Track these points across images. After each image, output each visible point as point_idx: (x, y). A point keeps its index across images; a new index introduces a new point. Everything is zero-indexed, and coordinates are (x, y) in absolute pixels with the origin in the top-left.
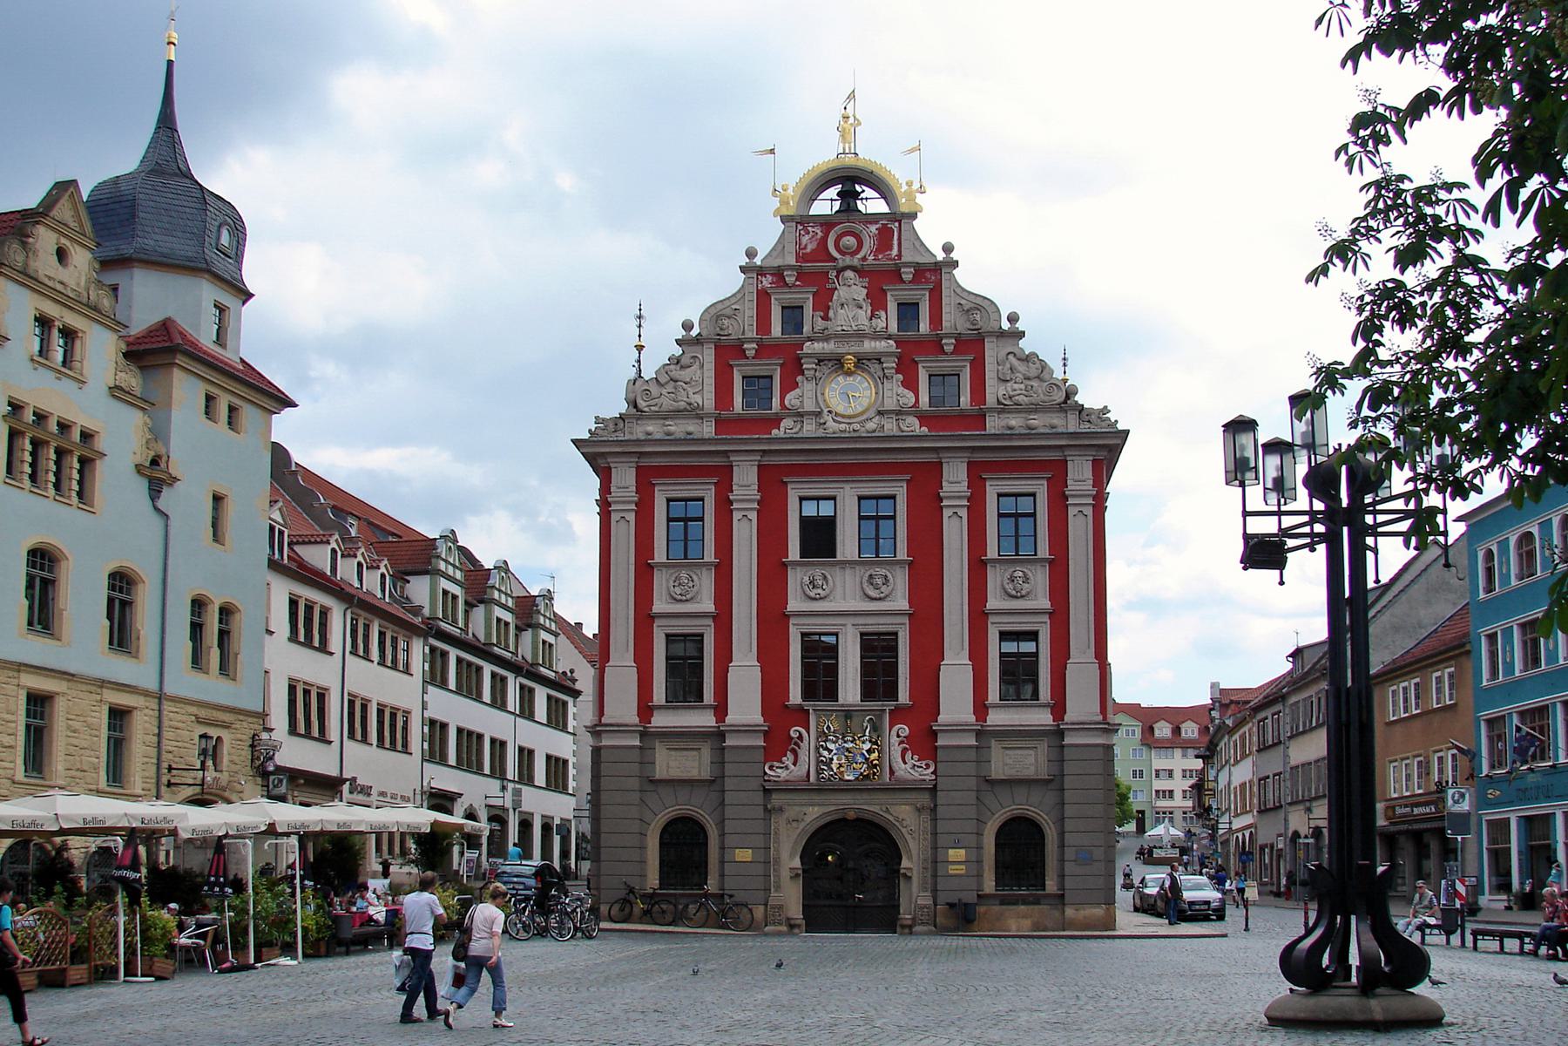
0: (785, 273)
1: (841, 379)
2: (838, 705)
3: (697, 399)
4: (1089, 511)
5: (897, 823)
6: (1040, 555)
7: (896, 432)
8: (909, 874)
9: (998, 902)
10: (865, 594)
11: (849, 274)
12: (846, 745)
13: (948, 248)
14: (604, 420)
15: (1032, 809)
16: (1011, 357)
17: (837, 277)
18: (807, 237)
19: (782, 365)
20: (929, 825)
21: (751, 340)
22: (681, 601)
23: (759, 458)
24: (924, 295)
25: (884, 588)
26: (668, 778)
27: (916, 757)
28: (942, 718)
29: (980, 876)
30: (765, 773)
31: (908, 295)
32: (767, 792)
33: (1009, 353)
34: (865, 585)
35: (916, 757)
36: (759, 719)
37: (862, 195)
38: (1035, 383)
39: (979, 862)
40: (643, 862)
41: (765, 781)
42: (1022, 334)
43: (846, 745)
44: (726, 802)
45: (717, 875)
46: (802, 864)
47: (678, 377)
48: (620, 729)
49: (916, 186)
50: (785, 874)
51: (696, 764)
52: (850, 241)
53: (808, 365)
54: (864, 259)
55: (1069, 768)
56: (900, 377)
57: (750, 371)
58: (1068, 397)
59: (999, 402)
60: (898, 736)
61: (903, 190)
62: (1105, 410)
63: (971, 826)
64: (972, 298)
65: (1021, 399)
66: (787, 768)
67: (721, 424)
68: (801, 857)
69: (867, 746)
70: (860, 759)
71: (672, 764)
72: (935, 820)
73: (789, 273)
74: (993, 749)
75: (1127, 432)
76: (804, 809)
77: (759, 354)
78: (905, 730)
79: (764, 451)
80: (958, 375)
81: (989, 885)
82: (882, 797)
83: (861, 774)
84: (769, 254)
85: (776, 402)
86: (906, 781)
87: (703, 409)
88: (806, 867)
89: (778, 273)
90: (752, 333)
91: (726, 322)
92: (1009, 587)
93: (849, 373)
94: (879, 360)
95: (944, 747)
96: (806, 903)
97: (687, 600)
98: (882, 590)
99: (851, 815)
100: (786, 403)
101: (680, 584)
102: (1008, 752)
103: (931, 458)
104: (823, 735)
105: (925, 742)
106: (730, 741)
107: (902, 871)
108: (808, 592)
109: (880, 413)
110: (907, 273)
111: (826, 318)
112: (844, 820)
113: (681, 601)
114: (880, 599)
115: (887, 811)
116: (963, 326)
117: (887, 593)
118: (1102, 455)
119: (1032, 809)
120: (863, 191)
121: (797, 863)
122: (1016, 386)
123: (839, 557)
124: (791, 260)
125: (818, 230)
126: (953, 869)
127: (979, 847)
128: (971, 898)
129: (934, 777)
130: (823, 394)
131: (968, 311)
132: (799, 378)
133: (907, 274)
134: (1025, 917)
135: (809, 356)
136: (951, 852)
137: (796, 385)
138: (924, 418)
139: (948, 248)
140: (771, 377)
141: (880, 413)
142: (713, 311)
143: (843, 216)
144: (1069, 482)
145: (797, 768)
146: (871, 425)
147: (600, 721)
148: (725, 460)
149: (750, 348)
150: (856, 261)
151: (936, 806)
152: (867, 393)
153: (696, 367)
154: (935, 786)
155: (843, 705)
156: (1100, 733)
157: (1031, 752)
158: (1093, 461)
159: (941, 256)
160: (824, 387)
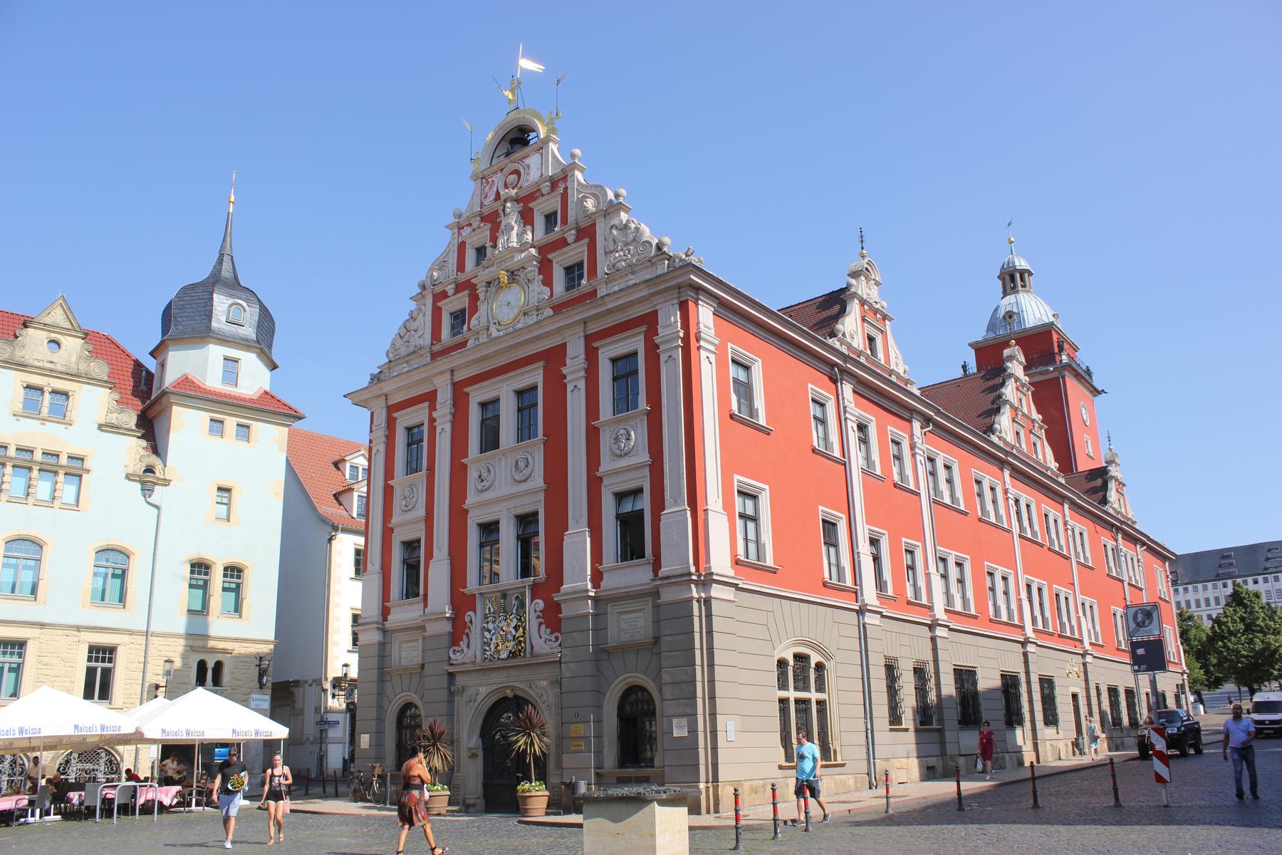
9: (615, 781)
17: (504, 210)
60: (536, 611)
69: (513, 624)
78: (540, 604)
95: (567, 618)
102: (624, 616)
105: (552, 618)
117: (528, 474)
157: (640, 614)
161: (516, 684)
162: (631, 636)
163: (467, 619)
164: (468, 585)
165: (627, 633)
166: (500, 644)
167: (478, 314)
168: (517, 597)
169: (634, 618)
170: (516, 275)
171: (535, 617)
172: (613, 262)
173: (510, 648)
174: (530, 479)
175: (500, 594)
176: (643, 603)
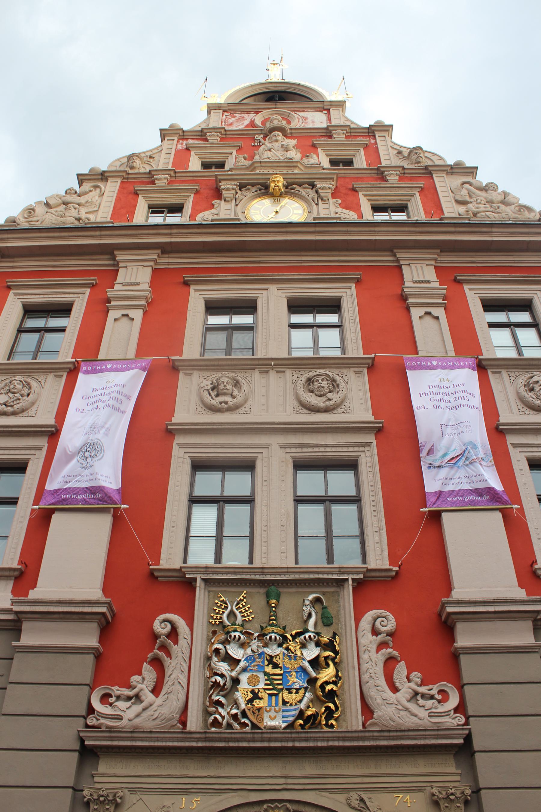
18: (233, 119)
24: (358, 151)
27: (416, 676)
30: (91, 710)
41: (87, 726)
43: (268, 651)
60: (375, 632)
69: (312, 652)
70: (297, 681)
86: (402, 732)
94: (313, 186)
117: (339, 400)
129: (462, 720)
132: (216, 202)
145: (159, 701)
154: (468, 738)
155: (262, 570)
164: (161, 562)
166: (264, 695)
168: (318, 600)
170: (293, 189)
171: (374, 647)
173: (302, 706)
174: (339, 410)
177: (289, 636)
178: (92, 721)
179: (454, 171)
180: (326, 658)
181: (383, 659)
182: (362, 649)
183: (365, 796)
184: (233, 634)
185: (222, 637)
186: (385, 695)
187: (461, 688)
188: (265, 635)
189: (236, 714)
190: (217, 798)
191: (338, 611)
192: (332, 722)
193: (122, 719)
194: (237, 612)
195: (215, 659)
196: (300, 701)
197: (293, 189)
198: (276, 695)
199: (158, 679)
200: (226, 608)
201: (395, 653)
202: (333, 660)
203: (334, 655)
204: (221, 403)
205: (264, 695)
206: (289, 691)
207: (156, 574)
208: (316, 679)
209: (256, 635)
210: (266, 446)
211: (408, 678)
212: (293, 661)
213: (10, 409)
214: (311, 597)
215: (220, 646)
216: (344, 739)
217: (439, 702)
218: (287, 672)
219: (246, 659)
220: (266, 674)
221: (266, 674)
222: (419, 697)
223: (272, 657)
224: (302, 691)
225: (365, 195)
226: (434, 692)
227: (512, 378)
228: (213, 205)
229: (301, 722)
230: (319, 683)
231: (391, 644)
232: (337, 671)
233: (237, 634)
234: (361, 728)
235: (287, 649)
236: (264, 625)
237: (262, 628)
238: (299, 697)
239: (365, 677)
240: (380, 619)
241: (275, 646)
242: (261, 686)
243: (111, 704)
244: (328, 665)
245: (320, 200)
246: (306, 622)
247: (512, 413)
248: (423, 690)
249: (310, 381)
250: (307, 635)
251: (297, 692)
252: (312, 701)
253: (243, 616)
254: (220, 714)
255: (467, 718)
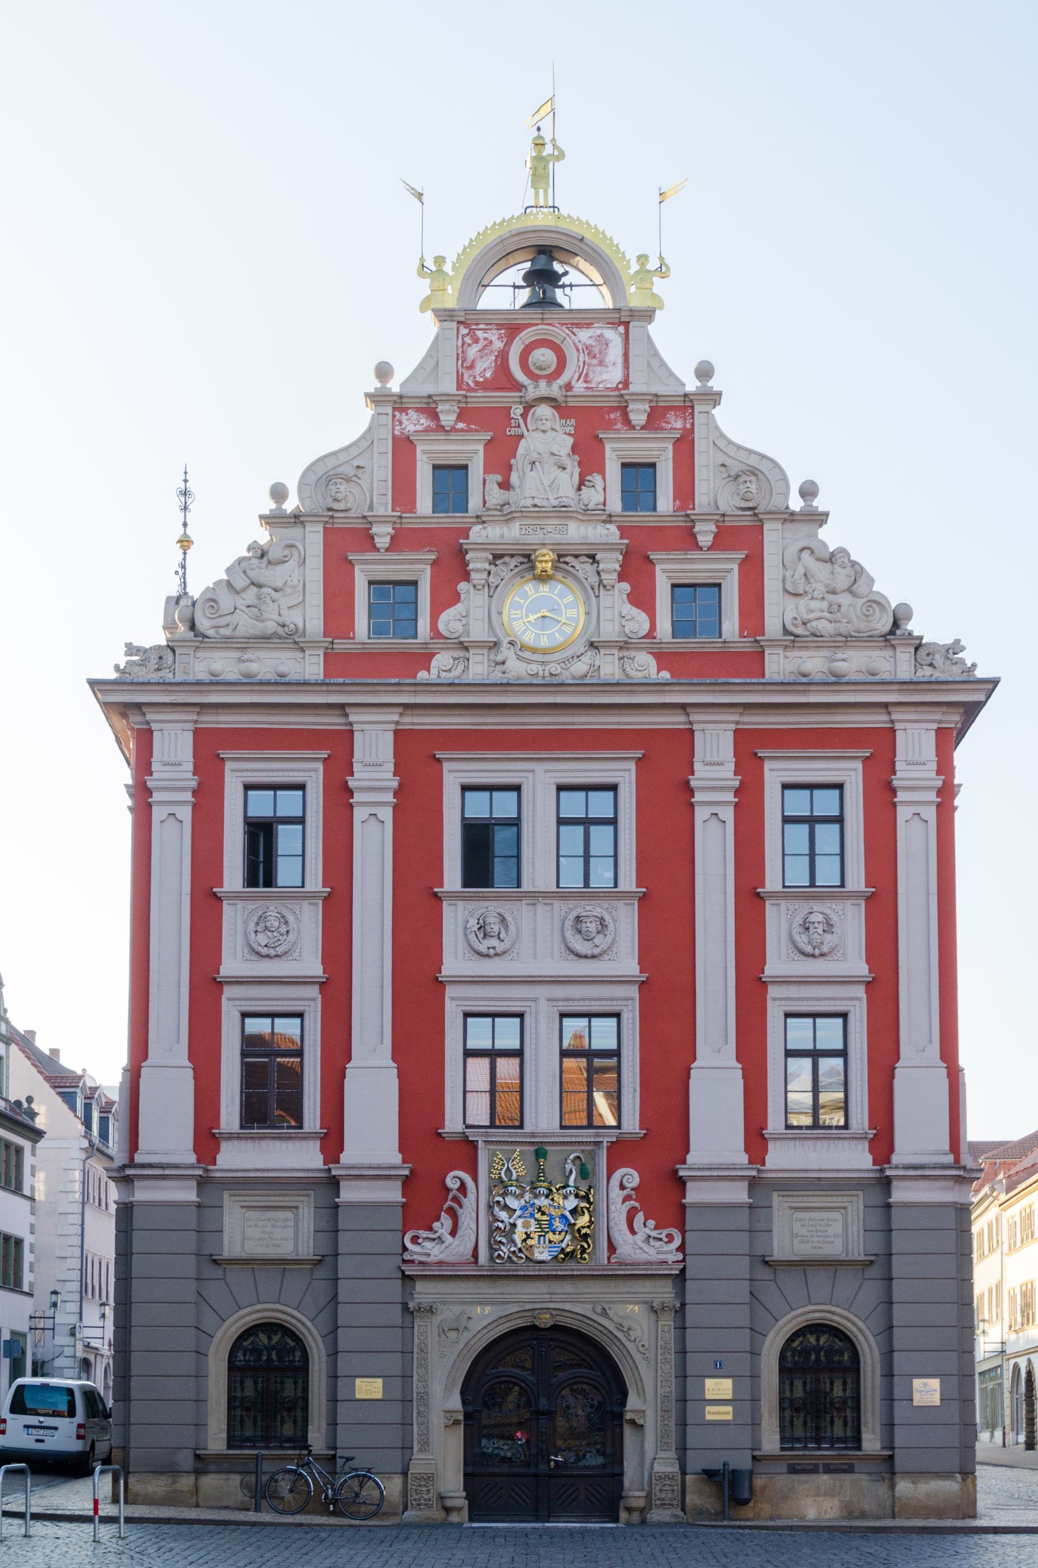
0: (440, 408)
1: (530, 588)
2: (525, 1135)
3: (294, 618)
4: (930, 813)
5: (620, 1335)
6: (851, 886)
7: (618, 676)
8: (640, 1422)
9: (785, 1470)
10: (568, 948)
11: (544, 411)
12: (537, 1202)
13: (704, 372)
14: (138, 650)
15: (839, 1310)
16: (806, 554)
17: (524, 416)
19: (434, 564)
20: (670, 1337)
21: (383, 520)
22: (268, 956)
23: (396, 718)
24: (664, 450)
25: (599, 939)
26: (244, 1256)
27: (651, 1223)
28: (690, 1159)
29: (755, 1424)
30: (405, 1249)
31: (641, 449)
32: (407, 1279)
33: (802, 550)
34: (569, 933)
35: (651, 1223)
36: (397, 1158)
37: (565, 280)
38: (845, 599)
39: (755, 1400)
40: (200, 1401)
41: (404, 1261)
42: (821, 518)
43: (537, 1202)
44: (340, 1299)
45: (324, 1425)
46: (464, 1402)
47: (262, 580)
48: (163, 1172)
49: (653, 264)
50: (437, 1420)
51: (290, 1232)
52: (544, 356)
53: (477, 562)
54: (568, 387)
55: (898, 1243)
56: (626, 587)
57: (382, 572)
58: (896, 624)
59: (786, 631)
60: (622, 1187)
61: (632, 271)
62: (956, 647)
63: (741, 1340)
64: (742, 456)
65: (824, 627)
66: (440, 1240)
67: (331, 658)
68: (462, 1393)
69: (572, 1203)
70: (558, 1225)
71: (250, 1232)
72: (682, 1328)
73: (447, 407)
74: (775, 1212)
75: (995, 682)
76: (469, 1308)
77: (397, 542)
78: (632, 1177)
79: (406, 706)
80: (719, 585)
81: (770, 1442)
82: (595, 1289)
83: (563, 1250)
84: (413, 377)
85: (424, 625)
87: (304, 635)
88: (470, 1409)
89: (429, 409)
90: (384, 507)
91: (343, 487)
92: (802, 940)
93: (543, 578)
94: (592, 557)
96: (470, 1470)
97: (277, 956)
98: (597, 941)
99: (545, 1321)
100: (441, 627)
101: (266, 928)
103: (675, 721)
104: (500, 1185)
106: (349, 1193)
107: (628, 1416)
108: (476, 944)
109: (592, 645)
110: (638, 411)
111: (505, 485)
112: (534, 1328)
113: (268, 956)
114: (593, 957)
115: (604, 1313)
116: (728, 502)
117: (604, 946)
118: (954, 719)
119: (839, 1310)
120: (566, 273)
121: (455, 1402)
122: (814, 604)
123: (526, 886)
124: (449, 386)
125: (493, 336)
126: (713, 1414)
127: (755, 1376)
128: (742, 1461)
129: (680, 1257)
130: (500, 613)
131: (737, 477)
132: (462, 586)
133: (638, 415)
134: (829, 1494)
135: (481, 547)
136: (710, 1383)
137: (455, 598)
138: (664, 659)
139: (704, 372)
140: (414, 583)
141: (592, 645)
142: (321, 470)
143: (535, 314)
144: (899, 766)
145: (457, 1240)
146: (579, 668)
147: (132, 1159)
148: (342, 720)
149: (382, 534)
150: (555, 390)
151: (683, 1305)
152: (572, 613)
153: (292, 563)
154: (683, 1271)
155: (533, 1135)
156: (951, 1183)
157: (837, 1215)
158: (938, 731)
159: (692, 385)
160: (502, 603)
161: (567, 1306)
162: (813, 1248)
163: (452, 1183)
164: (447, 1123)
165: (808, 1242)
167: (459, 607)
168: (578, 1157)
169: (822, 1220)
170: (567, 563)
171: (621, 1199)
172: (807, 617)
173: (564, 1245)
174: (606, 957)
175: (533, 1148)
176: (845, 1199)
177: (554, 1190)
178: (407, 1256)
179: (794, 518)
180: (582, 1208)
181: (627, 1209)
182: (611, 1202)
183: (606, 1307)
184: (510, 1189)
185: (501, 1192)
186: (626, 1238)
187: (683, 1232)
188: (535, 1188)
189: (514, 1251)
190: (501, 1307)
191: (594, 1166)
192: (586, 1256)
193: (430, 1255)
194: (512, 1169)
195: (496, 1209)
196: (562, 1241)
197: (567, 563)
198: (544, 1236)
199: (453, 1224)
200: (503, 1165)
201: (637, 1204)
202: (588, 1209)
203: (588, 1206)
204: (489, 948)
205: (536, 1236)
206: (554, 1232)
207: (443, 1135)
208: (574, 1224)
209: (528, 1188)
210: (535, 1000)
211: (645, 1225)
212: (557, 1210)
213: (272, 952)
214: (572, 1157)
215: (500, 1199)
216: (593, 1270)
217: (666, 1243)
218: (552, 1218)
219: (521, 1209)
220: (536, 1220)
221: (536, 1220)
222: (651, 1240)
223: (540, 1207)
224: (563, 1234)
225: (664, 571)
226: (663, 1236)
227: (790, 912)
228: (458, 595)
229: (563, 1256)
230: (577, 1227)
231: (634, 1197)
232: (591, 1217)
233: (513, 1189)
234: (606, 1262)
235: (553, 1200)
236: (534, 1180)
237: (532, 1183)
238: (561, 1237)
239: (612, 1224)
240: (627, 1177)
241: (543, 1198)
242: (532, 1229)
243: (419, 1244)
244: (583, 1212)
245: (601, 588)
246: (568, 1177)
247: (780, 959)
248: (654, 1234)
249: (578, 919)
250: (568, 1189)
251: (560, 1234)
252: (571, 1240)
253: (517, 1172)
254: (502, 1251)
255: (685, 1256)
